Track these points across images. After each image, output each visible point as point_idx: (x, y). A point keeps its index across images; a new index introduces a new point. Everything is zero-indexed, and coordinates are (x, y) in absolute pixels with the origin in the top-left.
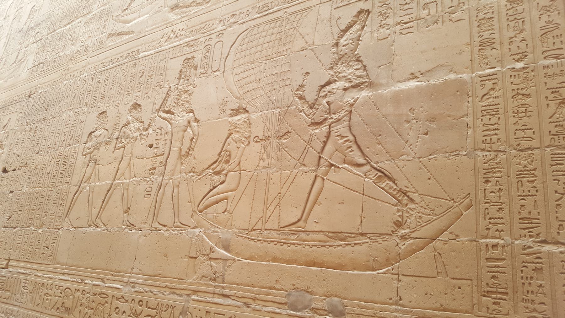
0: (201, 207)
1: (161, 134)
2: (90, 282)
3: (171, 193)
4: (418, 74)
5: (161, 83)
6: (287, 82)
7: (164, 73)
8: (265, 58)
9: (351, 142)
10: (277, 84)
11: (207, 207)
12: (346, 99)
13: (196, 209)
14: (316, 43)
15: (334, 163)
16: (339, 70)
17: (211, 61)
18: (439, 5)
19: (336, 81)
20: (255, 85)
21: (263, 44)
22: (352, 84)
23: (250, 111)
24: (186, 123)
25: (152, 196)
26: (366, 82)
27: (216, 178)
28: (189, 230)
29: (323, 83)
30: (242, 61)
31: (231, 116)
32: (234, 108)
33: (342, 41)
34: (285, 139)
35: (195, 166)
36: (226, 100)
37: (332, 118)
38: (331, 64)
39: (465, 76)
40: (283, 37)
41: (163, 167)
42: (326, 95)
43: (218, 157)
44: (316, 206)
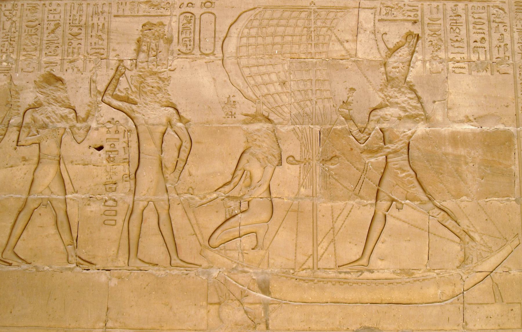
5: (102, 51)
6: (326, 94)
7: (105, 36)
9: (412, 177)
12: (402, 130)
14: (360, 55)
15: (396, 198)
16: (390, 94)
17: (197, 38)
18: (488, 53)
20: (279, 88)
22: (407, 114)
26: (422, 115)
32: (249, 113)
36: (232, 99)
37: (388, 148)
40: (313, 35)
44: (379, 244)
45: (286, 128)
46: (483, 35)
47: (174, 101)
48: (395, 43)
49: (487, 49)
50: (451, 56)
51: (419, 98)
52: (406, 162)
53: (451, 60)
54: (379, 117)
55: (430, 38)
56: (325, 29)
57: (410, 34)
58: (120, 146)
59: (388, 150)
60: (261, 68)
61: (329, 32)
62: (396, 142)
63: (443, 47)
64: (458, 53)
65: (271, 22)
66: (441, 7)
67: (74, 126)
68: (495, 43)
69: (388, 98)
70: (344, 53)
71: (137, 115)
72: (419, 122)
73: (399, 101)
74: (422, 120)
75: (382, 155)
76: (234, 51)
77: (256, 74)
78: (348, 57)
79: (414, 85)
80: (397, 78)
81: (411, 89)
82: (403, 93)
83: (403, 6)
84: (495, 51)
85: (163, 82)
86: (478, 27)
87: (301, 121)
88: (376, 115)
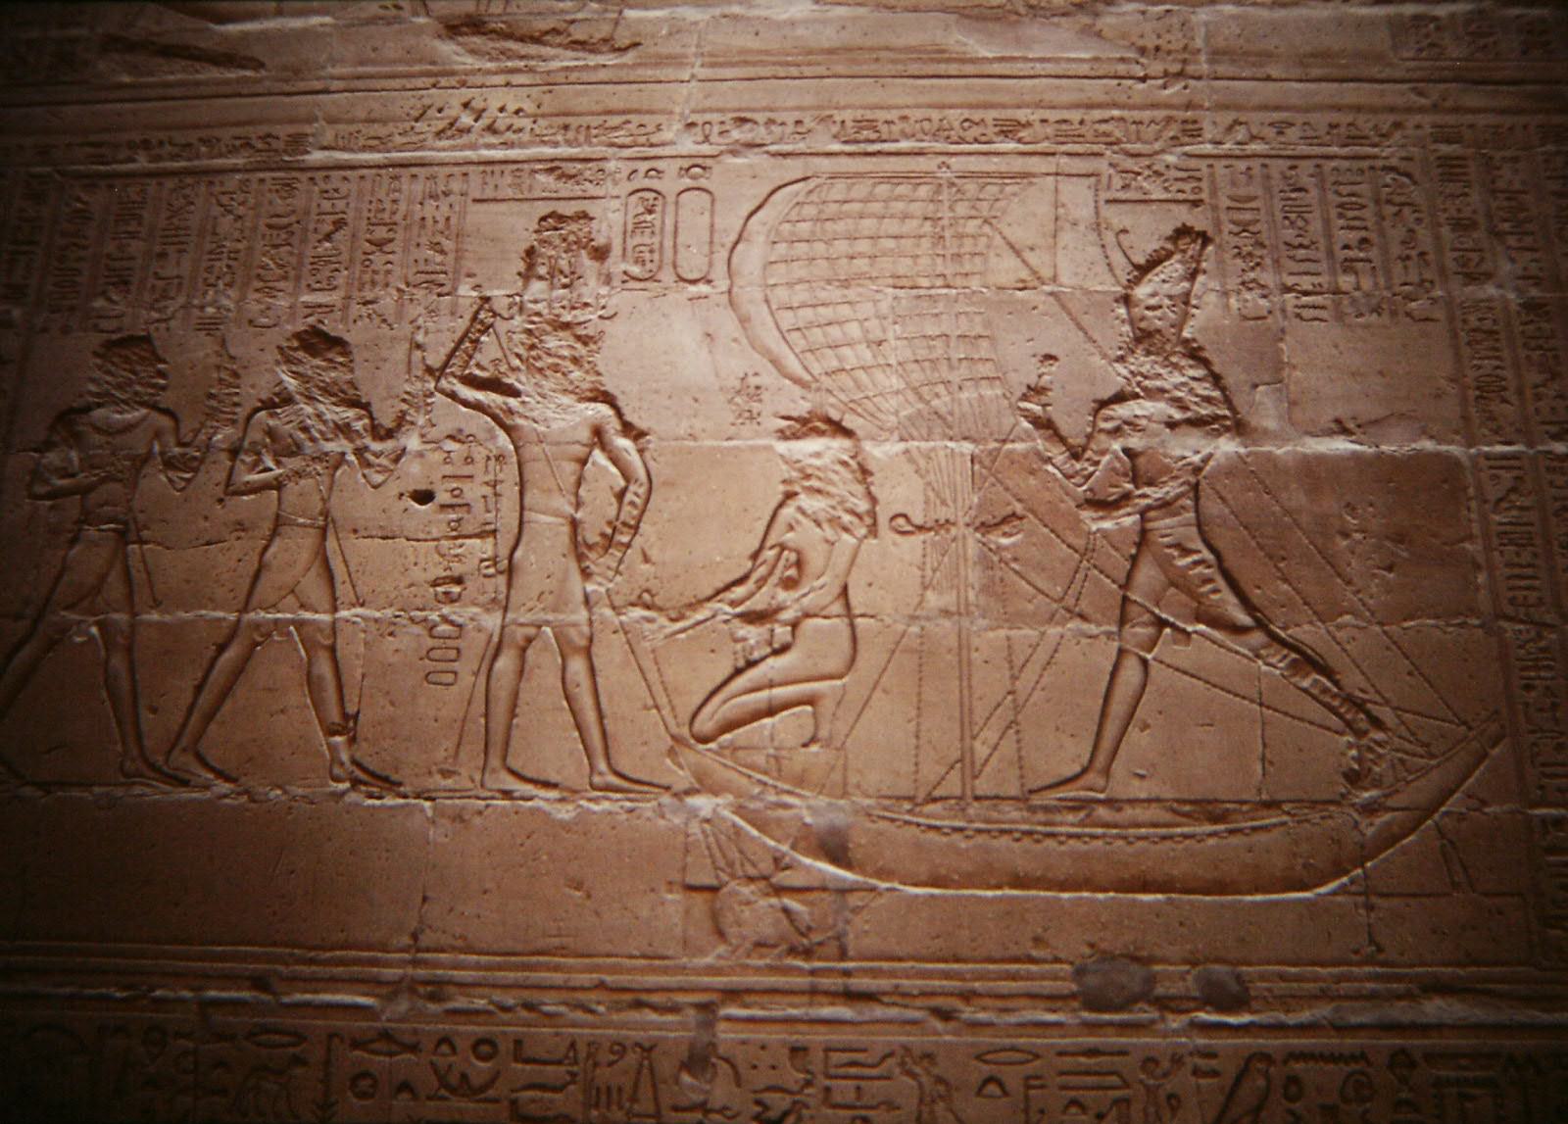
0: (705, 723)
1: (469, 460)
2: (187, 994)
4: (1351, 425)
6: (986, 370)
8: (891, 281)
10: (951, 368)
11: (730, 726)
12: (1178, 452)
13: (685, 731)
14: (1064, 279)
16: (1143, 370)
18: (1380, 273)
19: (1136, 396)
20: (867, 355)
22: (1189, 414)
23: (860, 433)
24: (585, 435)
25: (466, 679)
26: (1225, 417)
27: (753, 633)
28: (666, 799)
29: (1106, 394)
30: (799, 271)
31: (783, 435)
32: (795, 414)
33: (1141, 292)
34: (1005, 534)
35: (653, 584)
36: (753, 381)
37: (1144, 496)
39: (1455, 450)
40: (947, 234)
41: (502, 580)
43: (749, 564)
45: (887, 447)
46: (1363, 234)
47: (610, 388)
49: (1377, 263)
50: (1290, 281)
51: (1216, 379)
52: (1194, 529)
55: (1235, 240)
56: (978, 222)
57: (1183, 232)
58: (473, 492)
59: (1145, 502)
60: (821, 310)
61: (987, 229)
63: (1268, 261)
64: (1306, 273)
65: (846, 207)
66: (1257, 170)
67: (366, 448)
68: (1396, 250)
70: (1024, 274)
71: (520, 421)
73: (1167, 386)
74: (1228, 429)
76: (757, 272)
77: (810, 325)
79: (1200, 348)
80: (1158, 331)
81: (1195, 354)
82: (1175, 366)
84: (1398, 268)
85: (585, 344)
86: (1350, 214)
87: (924, 432)
88: (1112, 418)
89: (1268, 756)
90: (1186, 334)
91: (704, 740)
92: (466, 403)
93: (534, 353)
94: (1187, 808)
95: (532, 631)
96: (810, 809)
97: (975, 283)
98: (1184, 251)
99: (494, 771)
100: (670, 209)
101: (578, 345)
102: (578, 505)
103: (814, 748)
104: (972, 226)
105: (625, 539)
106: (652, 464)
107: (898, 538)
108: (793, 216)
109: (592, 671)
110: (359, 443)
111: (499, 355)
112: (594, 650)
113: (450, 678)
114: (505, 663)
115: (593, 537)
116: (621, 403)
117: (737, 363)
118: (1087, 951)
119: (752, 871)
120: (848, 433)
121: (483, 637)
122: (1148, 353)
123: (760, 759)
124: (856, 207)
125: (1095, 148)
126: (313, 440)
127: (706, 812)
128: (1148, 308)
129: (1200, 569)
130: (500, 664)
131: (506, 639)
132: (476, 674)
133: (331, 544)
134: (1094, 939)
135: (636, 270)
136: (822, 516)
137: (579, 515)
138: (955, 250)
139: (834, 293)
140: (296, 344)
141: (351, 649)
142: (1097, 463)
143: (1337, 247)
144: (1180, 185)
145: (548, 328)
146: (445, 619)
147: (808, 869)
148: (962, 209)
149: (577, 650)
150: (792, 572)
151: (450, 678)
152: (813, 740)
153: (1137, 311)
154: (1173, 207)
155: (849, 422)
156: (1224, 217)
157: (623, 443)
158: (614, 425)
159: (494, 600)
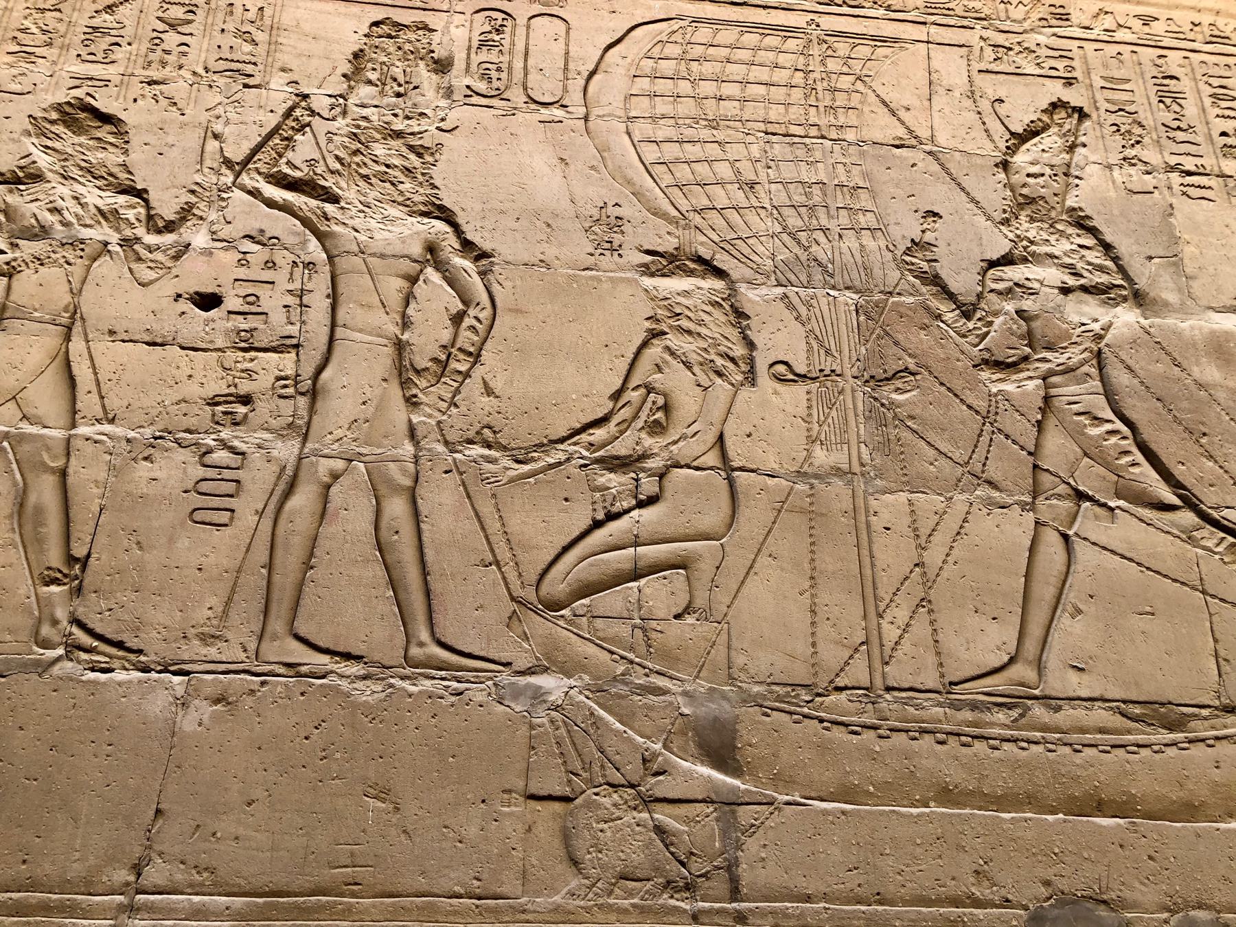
0: (556, 585)
3: (369, 516)
8: (762, 126)
12: (1076, 319)
14: (942, 139)
20: (740, 197)
21: (744, 83)
22: (1082, 281)
24: (416, 250)
27: (614, 481)
28: (505, 677)
30: (662, 107)
31: (646, 270)
35: (497, 421)
38: (1005, 211)
40: (819, 86)
41: (302, 402)
42: (1007, 293)
45: (764, 290)
47: (447, 203)
48: (1027, 121)
50: (1173, 160)
51: (1107, 247)
53: (1172, 169)
54: (1011, 284)
55: (1113, 118)
58: (273, 301)
60: (687, 146)
62: (1065, 348)
63: (1146, 140)
65: (711, 50)
66: (1126, 56)
67: (138, 240)
69: (1025, 243)
70: (901, 132)
72: (1118, 305)
73: (1057, 253)
74: (1125, 299)
75: (1031, 378)
76: (618, 102)
77: (677, 161)
78: (914, 142)
81: (1082, 223)
83: (1033, 48)
85: (420, 155)
86: (1224, 104)
87: (804, 278)
89: (1222, 653)
90: (1071, 202)
91: (554, 605)
92: (271, 204)
93: (357, 159)
94: (1137, 710)
95: (339, 465)
96: (686, 695)
97: (850, 136)
98: (1061, 126)
99: (275, 637)
100: (521, 31)
101: (412, 157)
102: (406, 324)
103: (690, 620)
104: (845, 82)
105: (463, 367)
106: (496, 288)
107: (779, 386)
108: (656, 52)
109: (416, 514)
110: (128, 233)
111: (317, 156)
112: (420, 491)
113: (224, 517)
114: (303, 500)
115: (422, 363)
116: (461, 220)
117: (595, 192)
118: (1043, 891)
119: (617, 778)
120: (720, 273)
121: (276, 469)
122: (1032, 220)
123: (623, 630)
124: (724, 52)
125: (965, 23)
126: (66, 224)
127: (556, 697)
128: (1028, 175)
129: (1114, 440)
130: (295, 502)
131: (303, 474)
132: (261, 514)
133: (77, 346)
134: (1049, 874)
135: (482, 86)
136: (693, 358)
137: (405, 337)
138: (828, 103)
139: (705, 134)
140: (54, 116)
141: (87, 474)
142: (990, 324)
143: (1215, 134)
144: (1053, 63)
145: (378, 136)
146: (224, 445)
147: (688, 775)
148: (832, 65)
149: (397, 489)
150: (659, 415)
151: (224, 517)
152: (688, 610)
153: (1017, 179)
154: (1047, 81)
155: (722, 261)
156: (1099, 96)
157: (459, 262)
158: (451, 241)
159: (290, 425)
